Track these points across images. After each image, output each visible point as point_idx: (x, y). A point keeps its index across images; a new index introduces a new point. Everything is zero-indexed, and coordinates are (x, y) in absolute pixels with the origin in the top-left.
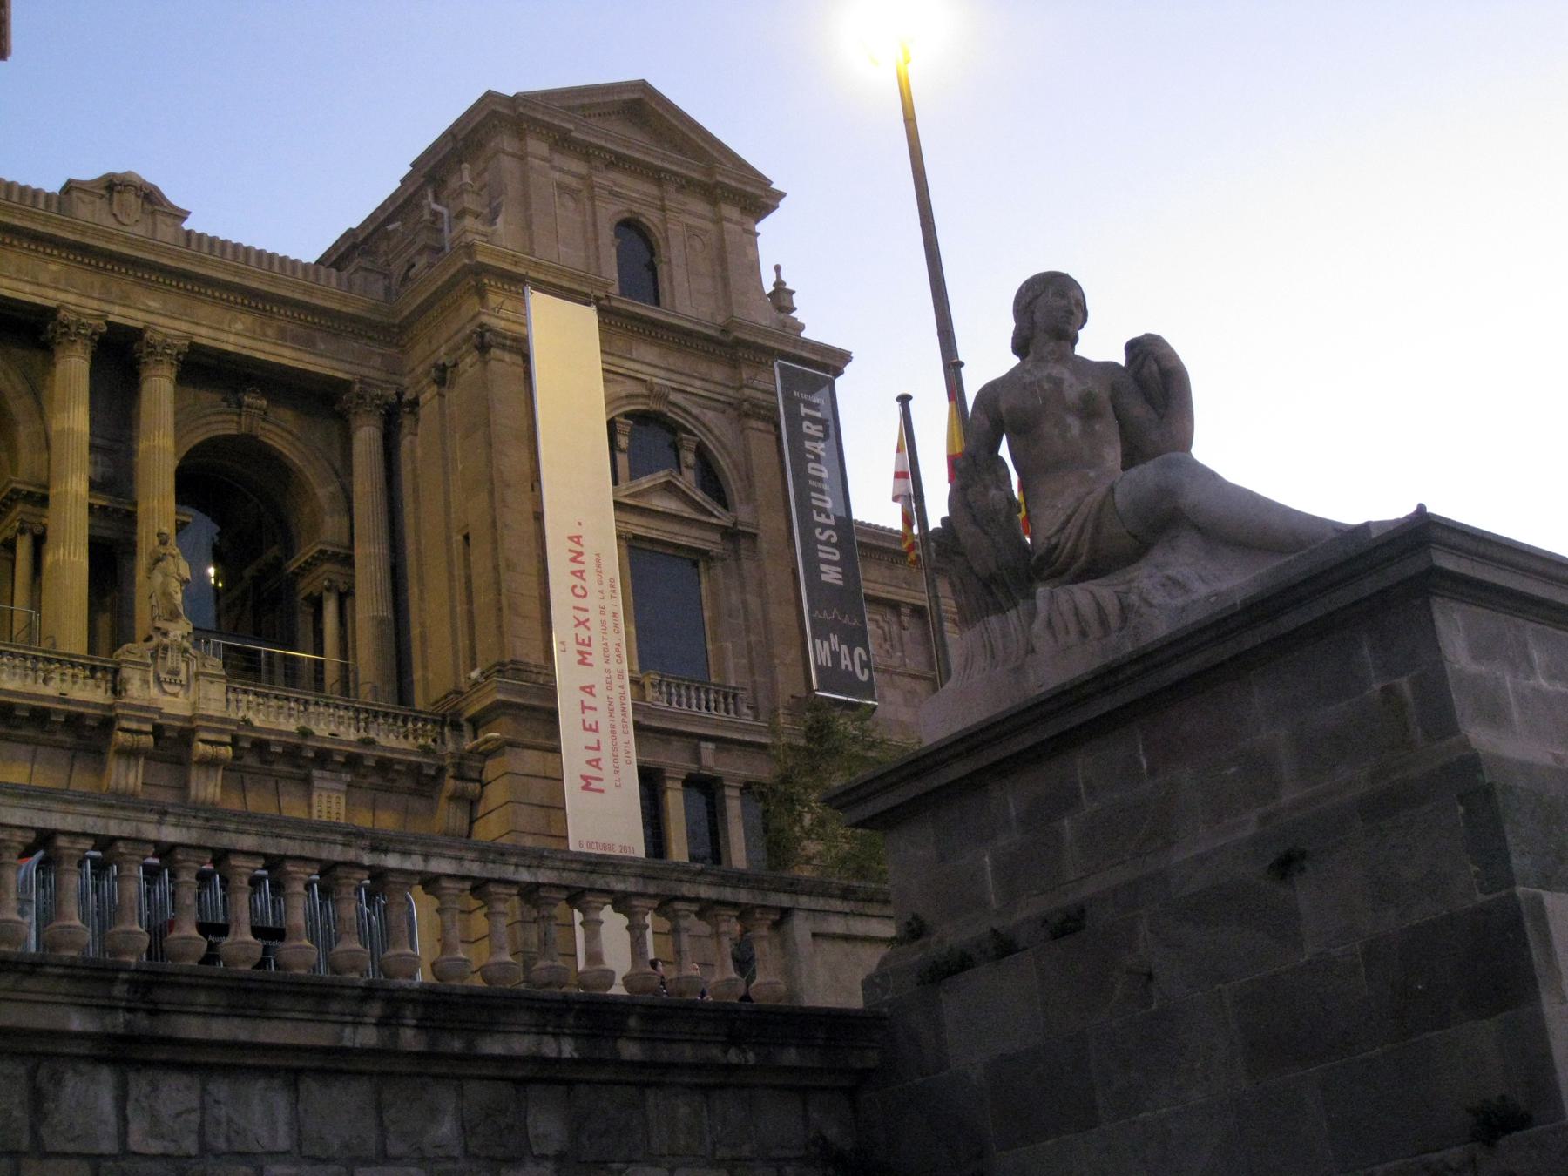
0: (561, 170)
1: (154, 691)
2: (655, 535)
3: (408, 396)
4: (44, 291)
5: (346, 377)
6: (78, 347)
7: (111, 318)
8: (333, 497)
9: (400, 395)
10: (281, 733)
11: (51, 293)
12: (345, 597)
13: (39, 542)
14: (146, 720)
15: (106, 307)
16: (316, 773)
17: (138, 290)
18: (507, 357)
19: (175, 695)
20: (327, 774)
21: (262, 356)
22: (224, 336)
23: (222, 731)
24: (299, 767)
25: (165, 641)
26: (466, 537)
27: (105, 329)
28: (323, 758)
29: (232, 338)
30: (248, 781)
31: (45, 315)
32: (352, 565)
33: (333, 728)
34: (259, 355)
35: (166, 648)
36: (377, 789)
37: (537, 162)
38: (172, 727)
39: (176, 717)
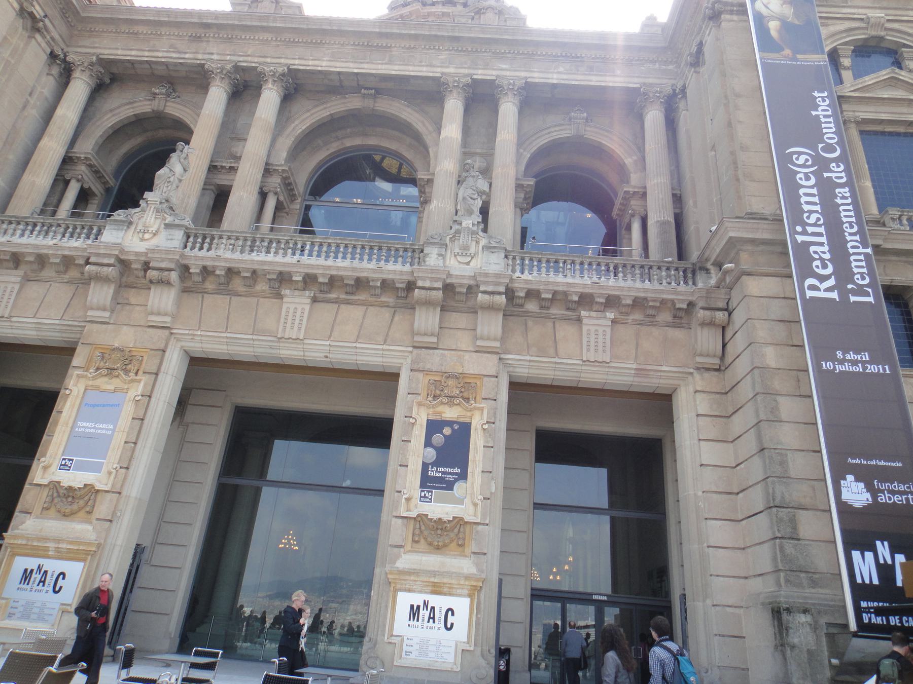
4: (435, 69)
5: (635, 86)
6: (455, 93)
7: (475, 77)
9: (674, 90)
10: (548, 283)
11: (439, 70)
14: (437, 279)
16: (584, 313)
19: (468, 263)
20: (593, 314)
21: (577, 83)
22: (550, 76)
23: (497, 284)
29: (555, 76)
30: (530, 323)
33: (595, 279)
36: (640, 323)
38: (461, 285)
39: (463, 277)
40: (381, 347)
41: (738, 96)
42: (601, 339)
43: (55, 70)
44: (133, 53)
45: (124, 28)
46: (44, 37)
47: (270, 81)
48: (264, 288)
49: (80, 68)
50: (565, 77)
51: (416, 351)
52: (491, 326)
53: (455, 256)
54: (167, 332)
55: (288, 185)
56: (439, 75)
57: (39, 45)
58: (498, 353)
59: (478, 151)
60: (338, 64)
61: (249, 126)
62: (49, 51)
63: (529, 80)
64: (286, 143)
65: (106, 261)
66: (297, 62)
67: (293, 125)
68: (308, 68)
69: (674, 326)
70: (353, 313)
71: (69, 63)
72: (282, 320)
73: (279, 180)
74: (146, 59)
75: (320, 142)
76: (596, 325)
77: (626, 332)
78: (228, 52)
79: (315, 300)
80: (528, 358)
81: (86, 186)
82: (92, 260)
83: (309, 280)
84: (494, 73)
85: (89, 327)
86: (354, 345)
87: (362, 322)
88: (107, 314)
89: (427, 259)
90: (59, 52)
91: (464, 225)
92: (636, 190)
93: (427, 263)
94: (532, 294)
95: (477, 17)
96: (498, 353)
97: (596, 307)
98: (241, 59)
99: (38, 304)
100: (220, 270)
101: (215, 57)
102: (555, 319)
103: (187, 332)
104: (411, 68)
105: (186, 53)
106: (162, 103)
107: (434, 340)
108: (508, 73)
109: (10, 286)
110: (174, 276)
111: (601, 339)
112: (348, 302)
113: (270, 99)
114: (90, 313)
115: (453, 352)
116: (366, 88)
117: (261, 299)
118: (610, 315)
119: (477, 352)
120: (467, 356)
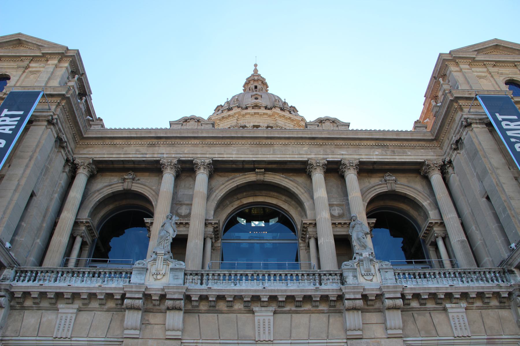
0: (477, 72)
1: (361, 280)
3: (447, 159)
7: (328, 159)
8: (429, 204)
10: (425, 288)
11: (305, 156)
12: (446, 239)
13: (316, 240)
15: (325, 156)
16: (448, 306)
17: (336, 149)
18: (479, 126)
19: (371, 280)
20: (454, 305)
22: (372, 157)
23: (395, 292)
24: (437, 304)
25: (361, 257)
26: (488, 198)
27: (326, 162)
29: (375, 157)
30: (416, 315)
31: (305, 163)
32: (444, 226)
33: (451, 283)
34: (386, 160)
35: (362, 261)
37: (466, 71)
39: (372, 290)
40: (325, 341)
41: (497, 169)
42: (461, 322)
43: (67, 169)
44: (114, 156)
45: (108, 142)
46: (65, 151)
47: (202, 168)
48: (240, 307)
49: (82, 167)
50: (381, 157)
51: (349, 342)
53: (363, 276)
54: (179, 342)
56: (306, 159)
57: (63, 156)
58: (401, 337)
59: (335, 203)
60: (242, 156)
61: (191, 197)
62: (66, 158)
63: (361, 160)
65: (137, 296)
66: (216, 156)
67: (215, 194)
68: (224, 159)
69: (501, 308)
71: (76, 164)
72: (257, 328)
73: (212, 230)
74: (122, 159)
75: (228, 202)
78: (172, 152)
79: (275, 313)
81: (85, 240)
82: (128, 295)
86: (307, 341)
87: (310, 325)
88: (137, 332)
89: (347, 280)
91: (364, 255)
92: (436, 221)
93: (348, 282)
94: (417, 296)
95: (320, 125)
96: (401, 337)
97: (454, 301)
98: (181, 156)
99: (89, 327)
100: (212, 297)
101: (165, 156)
102: (430, 310)
103: (192, 341)
104: (288, 156)
105: (146, 154)
106: (130, 184)
107: (360, 333)
108: (347, 156)
109: (69, 316)
111: (461, 322)
112: (297, 312)
113: (202, 177)
114: (126, 332)
115: (373, 340)
116: (258, 169)
117: (239, 315)
119: (388, 338)
120: (383, 342)
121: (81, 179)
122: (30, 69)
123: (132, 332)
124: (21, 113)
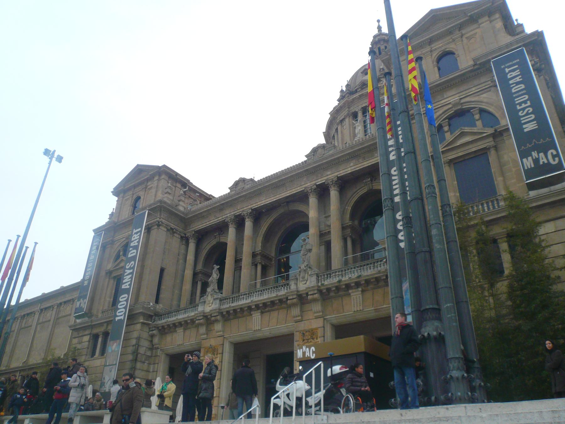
2: (460, 154)
10: (331, 284)
14: (294, 295)
16: (350, 291)
19: (306, 284)
20: (354, 290)
23: (314, 290)
28: (348, 287)
29: (349, 169)
38: (304, 294)
39: (303, 290)
43: (184, 242)
46: (177, 233)
50: (353, 168)
52: (317, 307)
55: (265, 257)
62: (180, 237)
64: (260, 239)
70: (274, 314)
76: (356, 294)
77: (369, 294)
79: (262, 313)
80: (334, 316)
83: (257, 307)
84: (325, 178)
85: (202, 341)
90: (183, 235)
101: (228, 215)
104: (294, 190)
107: (300, 318)
110: (219, 318)
112: (273, 310)
118: (360, 289)
120: (312, 321)
121: (192, 246)
122: (148, 187)
123: (204, 336)
124: (140, 229)
